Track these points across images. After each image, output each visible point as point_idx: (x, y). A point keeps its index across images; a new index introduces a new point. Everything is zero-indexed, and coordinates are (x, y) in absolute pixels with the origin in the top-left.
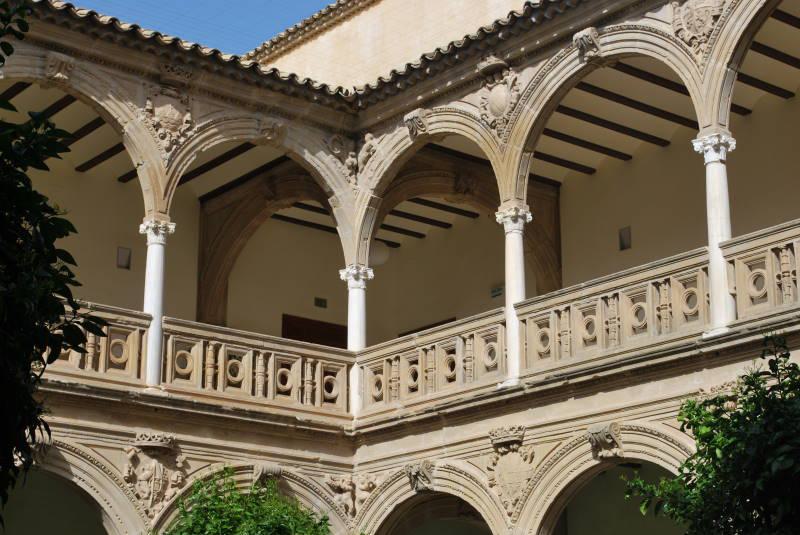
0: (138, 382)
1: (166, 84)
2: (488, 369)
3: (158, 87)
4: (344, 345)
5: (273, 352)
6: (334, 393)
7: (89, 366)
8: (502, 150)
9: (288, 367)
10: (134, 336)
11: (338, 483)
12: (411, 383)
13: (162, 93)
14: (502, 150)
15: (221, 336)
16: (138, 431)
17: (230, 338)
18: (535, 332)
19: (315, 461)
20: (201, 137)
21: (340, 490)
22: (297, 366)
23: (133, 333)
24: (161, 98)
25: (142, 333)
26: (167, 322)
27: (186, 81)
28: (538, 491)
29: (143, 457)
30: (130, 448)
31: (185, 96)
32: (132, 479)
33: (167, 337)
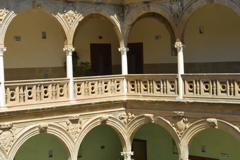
2: (171, 91)
3: (67, 4)
4: (121, 73)
5: (103, 81)
6: (119, 88)
8: (176, 25)
10: (65, 86)
12: (145, 88)
14: (176, 25)
15: (89, 80)
16: (70, 115)
17: (91, 80)
18: (187, 85)
19: (116, 111)
20: (79, 17)
21: (123, 118)
23: (65, 85)
25: (68, 84)
26: (74, 79)
28: (189, 132)
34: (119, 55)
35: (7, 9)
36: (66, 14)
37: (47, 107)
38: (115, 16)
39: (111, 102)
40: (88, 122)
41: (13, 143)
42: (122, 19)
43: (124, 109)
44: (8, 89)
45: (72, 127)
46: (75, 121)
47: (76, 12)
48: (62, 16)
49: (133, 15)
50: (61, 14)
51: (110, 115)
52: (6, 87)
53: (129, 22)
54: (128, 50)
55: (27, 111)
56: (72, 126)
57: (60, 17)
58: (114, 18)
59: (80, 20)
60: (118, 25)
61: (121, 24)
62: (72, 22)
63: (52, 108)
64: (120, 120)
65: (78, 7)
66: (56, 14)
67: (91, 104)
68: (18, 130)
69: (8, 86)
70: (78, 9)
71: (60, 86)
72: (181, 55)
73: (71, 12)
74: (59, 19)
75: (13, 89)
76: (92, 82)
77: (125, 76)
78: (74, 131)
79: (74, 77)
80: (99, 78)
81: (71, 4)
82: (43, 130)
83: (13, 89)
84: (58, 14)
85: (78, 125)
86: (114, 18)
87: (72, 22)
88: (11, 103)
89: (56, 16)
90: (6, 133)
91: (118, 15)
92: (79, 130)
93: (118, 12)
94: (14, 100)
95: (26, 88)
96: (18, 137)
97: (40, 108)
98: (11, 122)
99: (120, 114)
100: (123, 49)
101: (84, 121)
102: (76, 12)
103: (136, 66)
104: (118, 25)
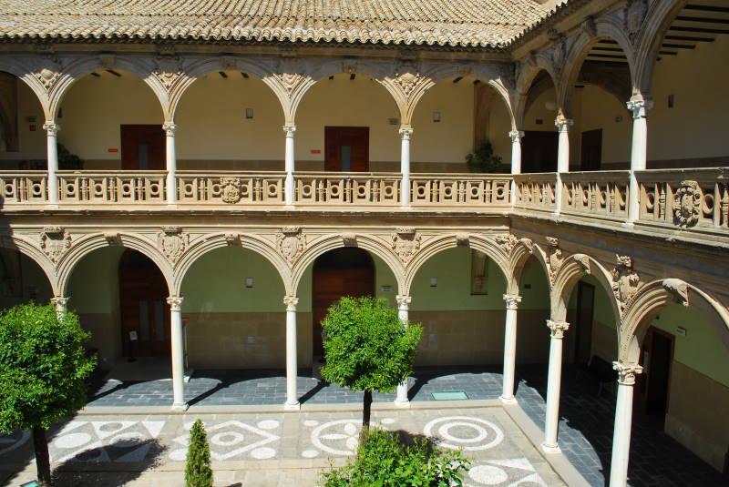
1: (405, 61)
3: (401, 63)
4: (510, 172)
9: (477, 186)
10: (396, 184)
11: (500, 239)
16: (397, 227)
21: (502, 242)
22: (482, 185)
24: (403, 68)
25: (399, 182)
27: (414, 58)
29: (399, 239)
30: (394, 234)
31: (415, 65)
32: (394, 248)
33: (412, 183)
34: (510, 142)
35: (301, 74)
37: (354, 211)
38: (499, 80)
39: (476, 214)
40: (431, 240)
42: (511, 84)
43: (508, 228)
44: (300, 182)
45: (402, 244)
46: (409, 237)
48: (391, 81)
49: (526, 75)
50: (392, 78)
51: (472, 235)
52: (296, 179)
53: (520, 90)
54: (523, 135)
55: (321, 213)
57: (389, 84)
58: (497, 83)
59: (428, 87)
60: (505, 94)
61: (509, 93)
62: (411, 89)
64: (497, 245)
66: (382, 79)
67: (435, 214)
68: (309, 238)
69: (300, 178)
70: (424, 70)
71: (386, 184)
72: (405, 145)
73: (408, 75)
74: (387, 86)
75: (307, 182)
76: (447, 182)
77: (514, 176)
78: (405, 250)
79: (411, 172)
80: (140, 174)
82: (463, 243)
83: (307, 182)
85: (414, 243)
86: (497, 83)
87: (411, 89)
88: (302, 201)
89: (383, 83)
90: (289, 239)
91: (504, 78)
92: (414, 251)
93: (503, 74)
94: (502, 199)
97: (342, 211)
98: (414, 227)
99: (497, 235)
100: (515, 133)
101: (424, 238)
103: (68, 161)
104: (505, 94)
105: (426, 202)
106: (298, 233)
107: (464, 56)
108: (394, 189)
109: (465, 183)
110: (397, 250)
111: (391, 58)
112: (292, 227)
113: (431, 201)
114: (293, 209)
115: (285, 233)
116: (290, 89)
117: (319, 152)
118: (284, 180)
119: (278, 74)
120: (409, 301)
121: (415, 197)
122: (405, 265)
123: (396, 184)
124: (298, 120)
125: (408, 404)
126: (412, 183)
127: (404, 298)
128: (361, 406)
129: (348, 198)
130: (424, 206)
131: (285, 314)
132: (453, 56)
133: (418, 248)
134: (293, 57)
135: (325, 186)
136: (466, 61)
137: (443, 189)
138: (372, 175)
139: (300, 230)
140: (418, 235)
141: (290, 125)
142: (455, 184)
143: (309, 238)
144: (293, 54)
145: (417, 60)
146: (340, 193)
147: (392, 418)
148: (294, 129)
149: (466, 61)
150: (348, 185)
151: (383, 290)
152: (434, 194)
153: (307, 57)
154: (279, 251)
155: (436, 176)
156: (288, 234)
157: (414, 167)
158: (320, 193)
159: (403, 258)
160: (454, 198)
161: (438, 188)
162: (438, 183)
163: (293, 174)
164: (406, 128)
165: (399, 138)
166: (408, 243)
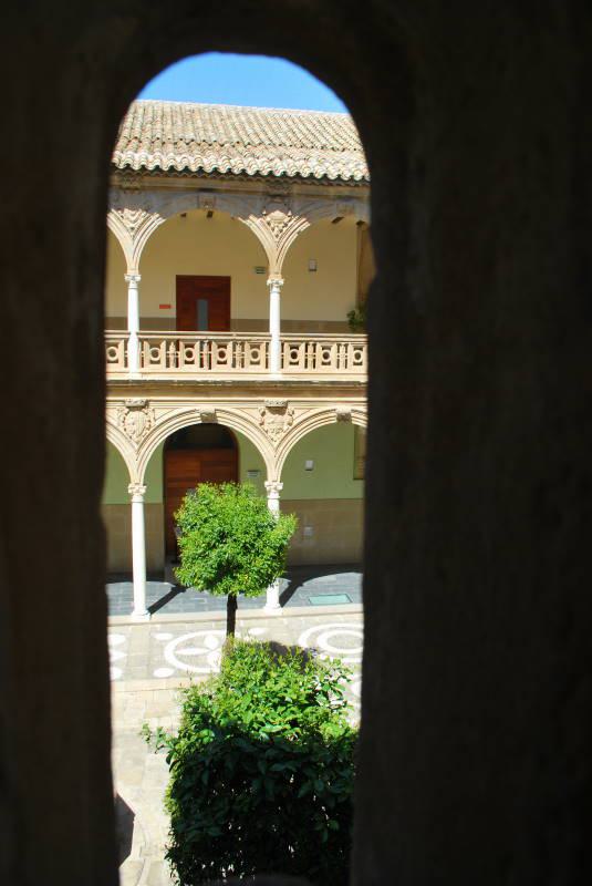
0: (266, 371)
1: (275, 196)
3: (269, 199)
7: (237, 366)
10: (263, 346)
13: (272, 202)
16: (266, 399)
24: (271, 205)
25: (267, 344)
29: (268, 414)
30: (262, 407)
31: (286, 201)
32: (261, 424)
33: (283, 345)
35: (147, 211)
36: (268, 219)
41: (148, 432)
46: (280, 410)
47: (290, 214)
48: (258, 221)
52: (141, 341)
55: (172, 382)
56: (270, 417)
57: (255, 224)
59: (302, 228)
63: (223, 382)
65: (296, 206)
66: (246, 218)
68: (159, 413)
69: (146, 340)
70: (297, 208)
71: (252, 347)
72: (275, 299)
73: (278, 214)
75: (155, 344)
76: (324, 344)
79: (282, 331)
81: (277, 200)
83: (155, 344)
84: (251, 217)
85: (286, 418)
87: (281, 231)
88: (149, 368)
89: (247, 222)
90: (134, 415)
92: (285, 427)
95: (181, 344)
96: (158, 423)
97: (199, 379)
98: (286, 399)
101: (297, 413)
102: (290, 214)
105: (300, 368)
106: (143, 407)
107: (345, 191)
108: (261, 353)
109: (346, 346)
110: (266, 427)
111: (255, 192)
112: (137, 400)
113: (306, 367)
114: (138, 377)
115: (128, 407)
116: (132, 229)
117: (169, 307)
118: (126, 341)
119: (118, 209)
120: (280, 488)
121: (286, 363)
122: (276, 444)
123: (263, 346)
124: (142, 268)
125: (281, 611)
126: (283, 345)
127: (275, 484)
128: (224, 614)
129: (205, 363)
130: (297, 373)
131: (129, 507)
132: (332, 191)
133: (290, 424)
134: (137, 189)
135: (178, 349)
136: (348, 198)
137: (320, 352)
138: (234, 335)
139: (146, 404)
140: (290, 408)
141: (133, 274)
142: (334, 347)
143: (159, 413)
144: (136, 184)
145: (288, 195)
146: (196, 357)
147: (260, 626)
148: (138, 278)
149: (348, 198)
150: (206, 346)
151: (248, 474)
152: (310, 359)
153: (154, 189)
154: (122, 429)
155: (311, 337)
156: (132, 408)
157: (286, 326)
158: (172, 358)
159: (273, 436)
160: (334, 363)
161: (315, 351)
162: (314, 345)
163: (138, 334)
164: (275, 279)
165: (267, 291)
166: (278, 417)
